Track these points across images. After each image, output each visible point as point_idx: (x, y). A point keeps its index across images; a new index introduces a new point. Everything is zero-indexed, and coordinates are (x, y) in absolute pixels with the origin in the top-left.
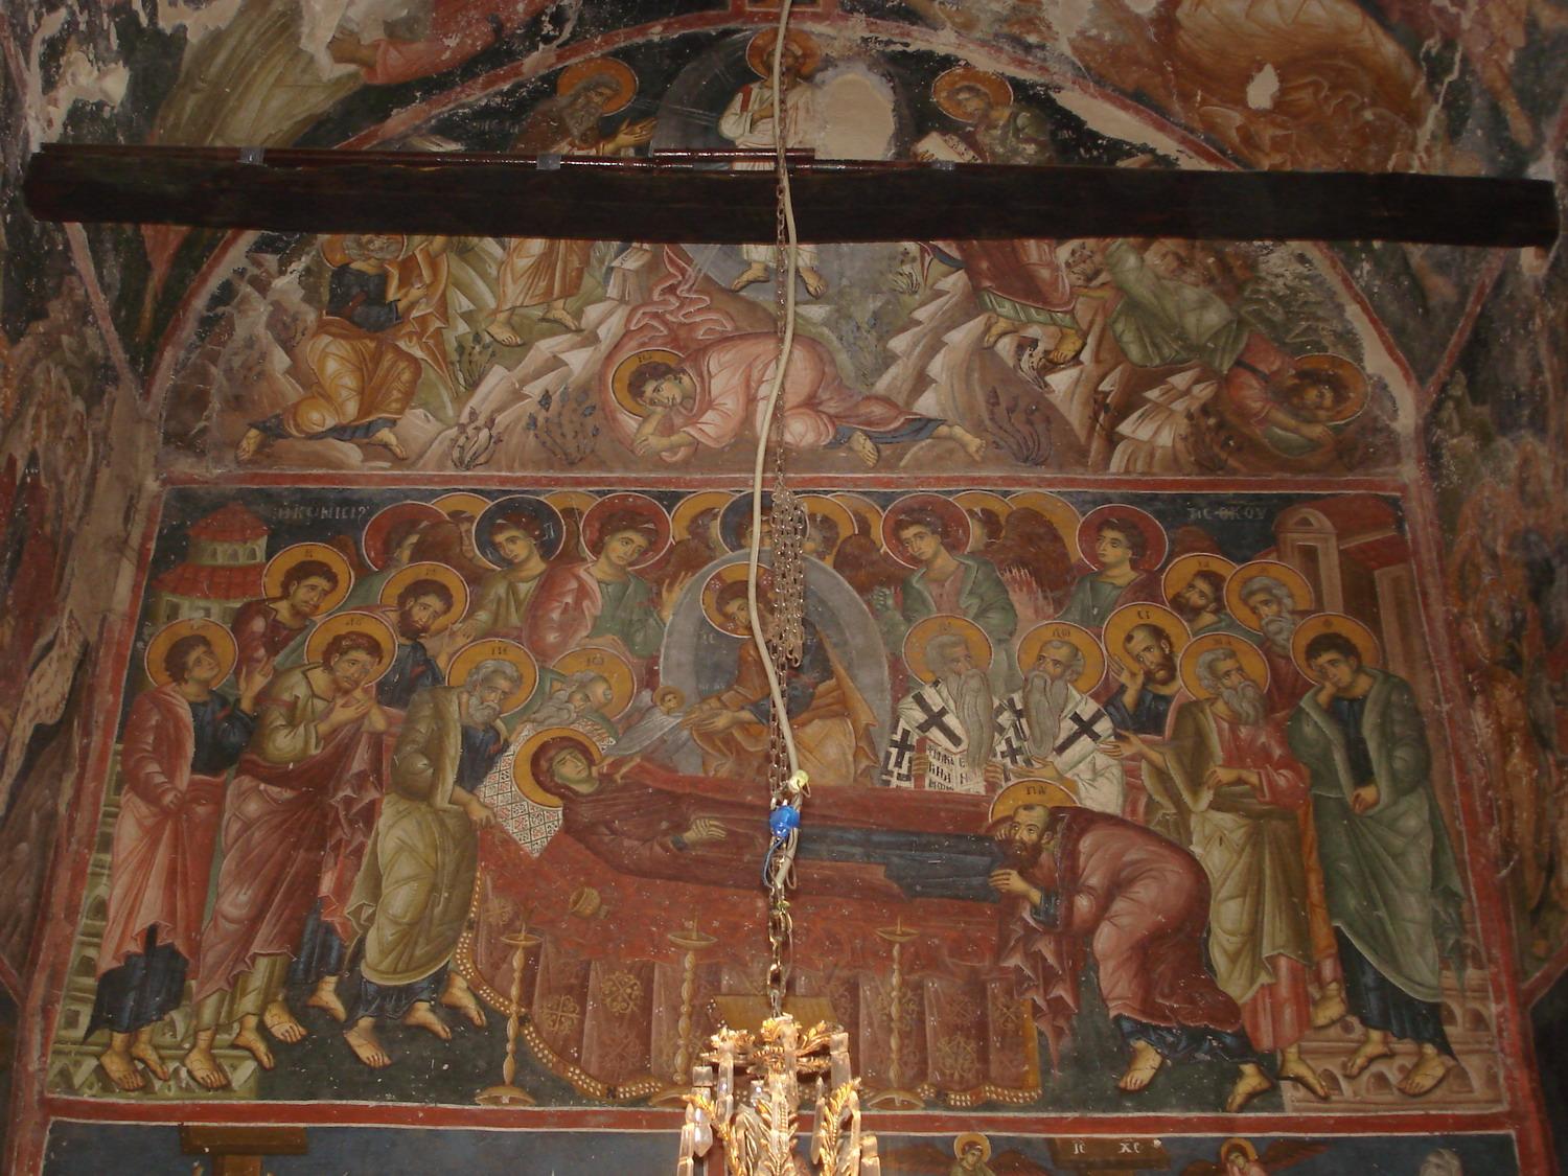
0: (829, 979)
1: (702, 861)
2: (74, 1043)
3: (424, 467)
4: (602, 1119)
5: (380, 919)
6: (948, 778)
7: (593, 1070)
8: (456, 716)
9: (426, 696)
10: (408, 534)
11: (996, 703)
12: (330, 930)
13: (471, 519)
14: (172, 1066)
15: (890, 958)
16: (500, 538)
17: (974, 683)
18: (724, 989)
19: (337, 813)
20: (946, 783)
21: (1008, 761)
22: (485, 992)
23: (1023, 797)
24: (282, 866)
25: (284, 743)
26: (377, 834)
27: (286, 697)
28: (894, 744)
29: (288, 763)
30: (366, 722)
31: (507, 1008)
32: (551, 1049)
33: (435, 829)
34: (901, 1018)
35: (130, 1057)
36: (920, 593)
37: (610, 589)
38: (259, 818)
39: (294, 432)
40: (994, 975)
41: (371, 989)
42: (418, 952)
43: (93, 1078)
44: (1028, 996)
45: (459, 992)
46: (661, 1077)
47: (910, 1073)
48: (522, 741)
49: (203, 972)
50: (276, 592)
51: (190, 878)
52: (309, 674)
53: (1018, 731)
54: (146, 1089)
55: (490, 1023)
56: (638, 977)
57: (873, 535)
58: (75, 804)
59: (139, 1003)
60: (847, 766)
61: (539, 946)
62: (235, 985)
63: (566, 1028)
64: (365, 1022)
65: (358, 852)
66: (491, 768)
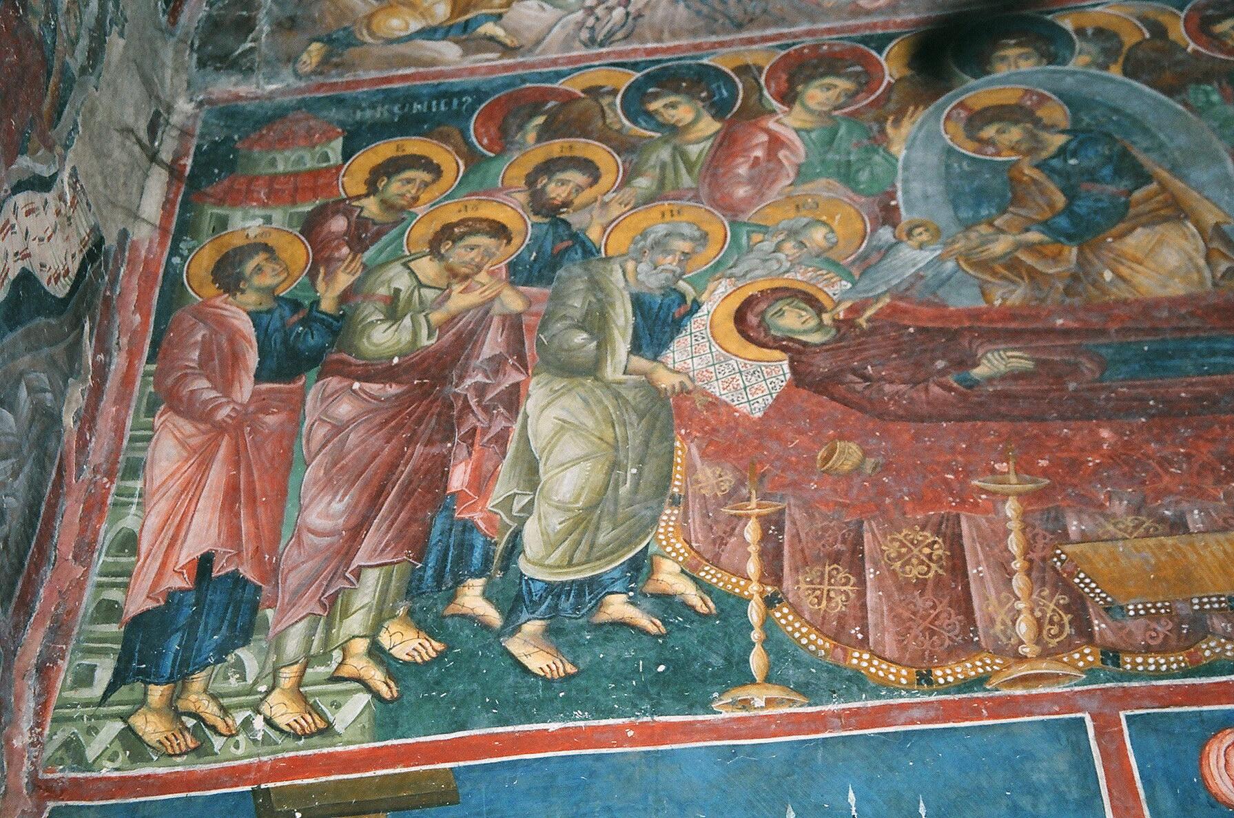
2: (86, 705)
3: (544, 52)
4: (916, 713)
5: (541, 507)
7: (891, 650)
8: (622, 284)
9: (577, 270)
10: (531, 116)
13: (614, 92)
14: (240, 717)
16: (655, 106)
24: (393, 467)
25: (382, 338)
26: (526, 417)
27: (383, 291)
30: (496, 308)
35: (174, 711)
37: (813, 135)
38: (354, 419)
39: (368, 39)
41: (539, 585)
42: (602, 538)
43: (117, 746)
45: (669, 576)
46: (998, 651)
48: (718, 300)
49: (283, 598)
50: (363, 190)
51: (259, 492)
52: (412, 265)
54: (202, 750)
55: (722, 610)
56: (937, 533)
57: (1172, 36)
58: (88, 419)
59: (186, 647)
60: (1199, 270)
61: (781, 512)
62: (334, 607)
64: (533, 627)
65: (501, 439)
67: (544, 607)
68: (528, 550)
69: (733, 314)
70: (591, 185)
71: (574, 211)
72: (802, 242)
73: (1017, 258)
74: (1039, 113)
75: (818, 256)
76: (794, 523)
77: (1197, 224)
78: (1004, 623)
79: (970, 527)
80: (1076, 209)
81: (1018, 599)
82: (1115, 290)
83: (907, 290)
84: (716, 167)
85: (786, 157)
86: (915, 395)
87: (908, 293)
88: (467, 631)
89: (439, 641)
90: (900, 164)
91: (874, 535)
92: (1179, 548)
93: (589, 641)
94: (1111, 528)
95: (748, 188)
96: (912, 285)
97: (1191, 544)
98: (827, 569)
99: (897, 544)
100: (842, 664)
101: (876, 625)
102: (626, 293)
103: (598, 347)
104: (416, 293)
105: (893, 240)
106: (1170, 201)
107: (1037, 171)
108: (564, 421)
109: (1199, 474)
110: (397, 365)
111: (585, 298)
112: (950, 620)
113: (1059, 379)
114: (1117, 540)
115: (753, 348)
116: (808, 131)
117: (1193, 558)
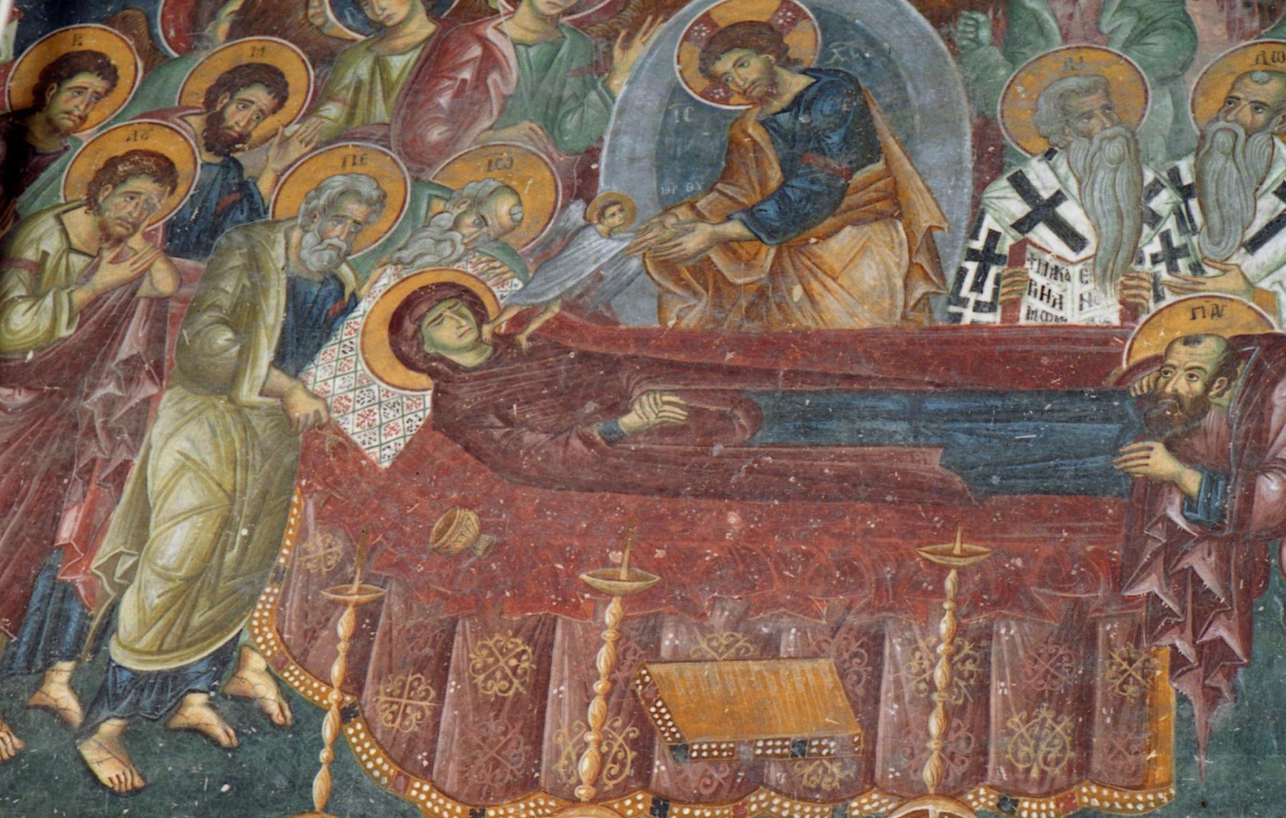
0: (835, 631)
1: (645, 457)
5: (145, 574)
6: (1058, 303)
7: (451, 783)
8: (281, 264)
9: (238, 237)
11: (1149, 176)
12: (68, 592)
15: (941, 592)
17: (1114, 149)
18: (665, 652)
19: (92, 417)
20: (1055, 312)
21: (1162, 268)
22: (293, 675)
23: (1183, 324)
26: (149, 448)
27: (30, 255)
28: (972, 255)
29: (25, 352)
30: (145, 290)
31: (325, 696)
32: (389, 756)
33: (236, 435)
34: (949, 686)
36: (1035, 15)
37: (532, 52)
40: (1113, 609)
41: (126, 675)
42: (197, 620)
44: (1165, 641)
47: (957, 770)
48: (377, 294)
52: (65, 218)
53: (1183, 218)
55: (297, 722)
56: (529, 640)
60: (892, 297)
63: (413, 722)
64: (110, 727)
66: (328, 338)
67: (124, 704)
68: (121, 630)
69: (389, 317)
70: (274, 111)
71: (250, 148)
72: (483, 217)
73: (709, 258)
74: (787, 40)
75: (496, 240)
76: (389, 616)
77: (908, 228)
78: (569, 758)
79: (563, 634)
80: (789, 191)
81: (589, 729)
82: (799, 316)
83: (581, 296)
84: (417, 92)
85: (497, 87)
86: (552, 450)
87: (581, 302)
88: (47, 728)
89: (19, 737)
90: (615, 108)
91: (465, 639)
92: (763, 678)
93: (161, 749)
94: (704, 645)
95: (443, 129)
96: (587, 290)
97: (776, 673)
98: (410, 678)
99: (485, 652)
100: (400, 795)
101: (444, 751)
102: (283, 276)
103: (240, 353)
104: (64, 261)
105: (582, 222)
106: (890, 190)
107: (762, 130)
108: (187, 457)
109: (811, 580)
110: (30, 363)
111: (239, 279)
112: (518, 750)
113: (708, 438)
114: (706, 661)
115: (401, 368)
116: (528, 46)
117: (773, 690)
